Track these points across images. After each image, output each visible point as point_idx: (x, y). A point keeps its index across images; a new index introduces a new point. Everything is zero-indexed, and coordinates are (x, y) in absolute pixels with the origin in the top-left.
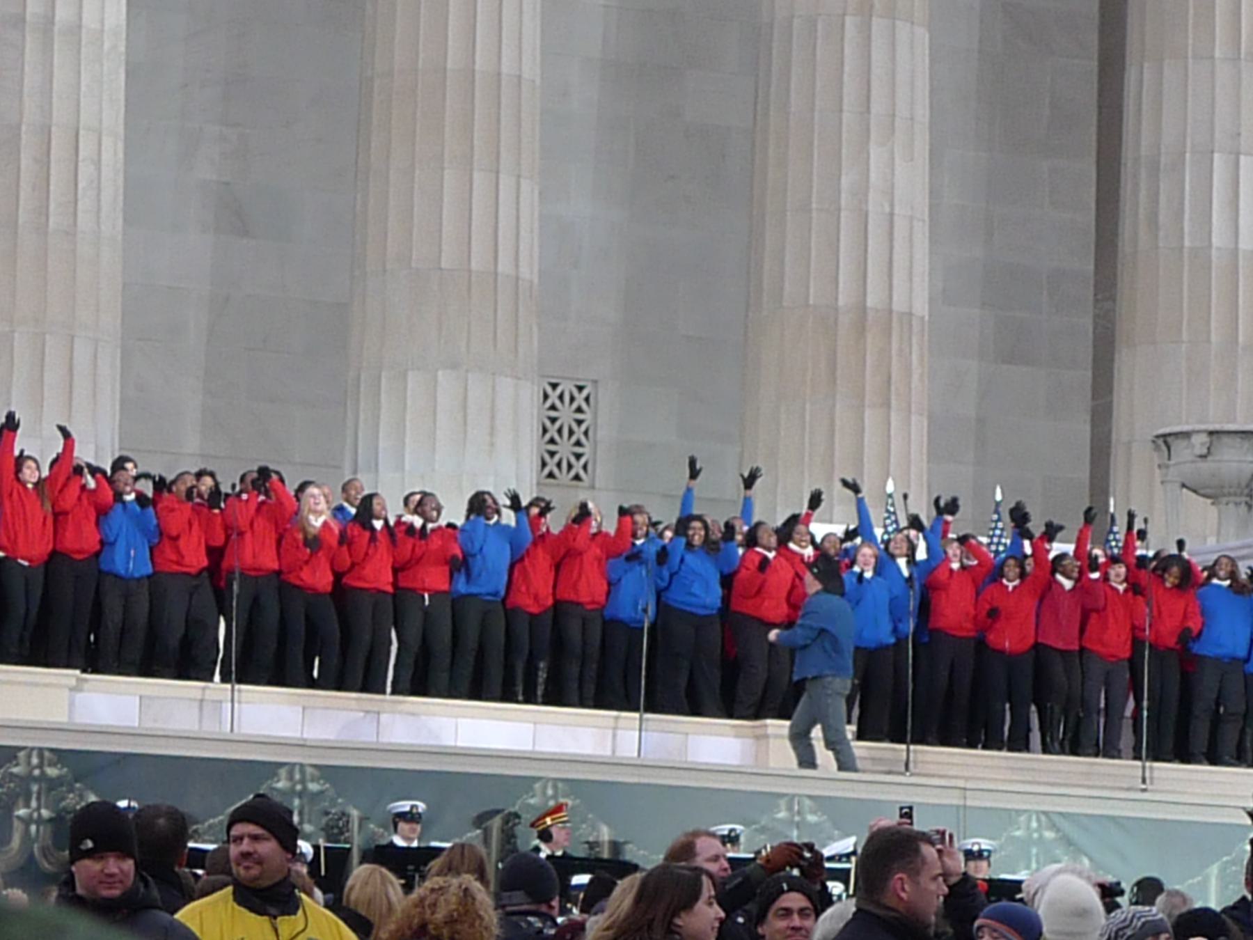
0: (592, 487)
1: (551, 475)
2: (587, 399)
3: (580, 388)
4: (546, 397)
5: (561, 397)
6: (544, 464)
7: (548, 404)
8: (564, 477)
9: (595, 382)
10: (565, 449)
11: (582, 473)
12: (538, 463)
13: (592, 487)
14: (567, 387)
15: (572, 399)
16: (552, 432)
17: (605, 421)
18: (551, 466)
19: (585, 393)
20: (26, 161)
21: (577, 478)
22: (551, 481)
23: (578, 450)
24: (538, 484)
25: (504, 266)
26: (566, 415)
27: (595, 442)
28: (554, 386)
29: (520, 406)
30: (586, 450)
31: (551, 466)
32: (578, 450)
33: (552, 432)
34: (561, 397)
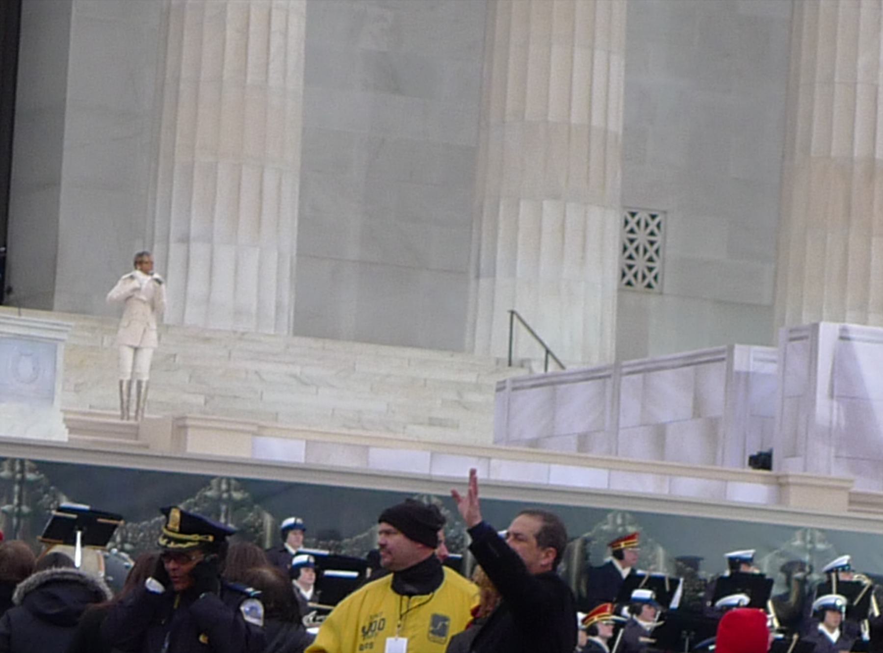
0: (661, 293)
1: (629, 283)
2: (658, 226)
3: (653, 217)
4: (626, 223)
5: (638, 223)
6: (624, 275)
7: (628, 228)
8: (640, 285)
9: (665, 212)
10: (640, 263)
11: (653, 283)
12: (617, 274)
13: (661, 293)
14: (643, 216)
15: (647, 225)
16: (631, 250)
17: (672, 243)
18: (629, 276)
19: (657, 220)
20: (230, 33)
21: (649, 286)
22: (629, 287)
23: (650, 264)
24: (620, 290)
25: (597, 120)
26: (642, 237)
27: (664, 259)
28: (633, 215)
29: (605, 230)
30: (657, 265)
31: (629, 276)
32: (650, 264)
33: (631, 250)
34: (638, 223)
